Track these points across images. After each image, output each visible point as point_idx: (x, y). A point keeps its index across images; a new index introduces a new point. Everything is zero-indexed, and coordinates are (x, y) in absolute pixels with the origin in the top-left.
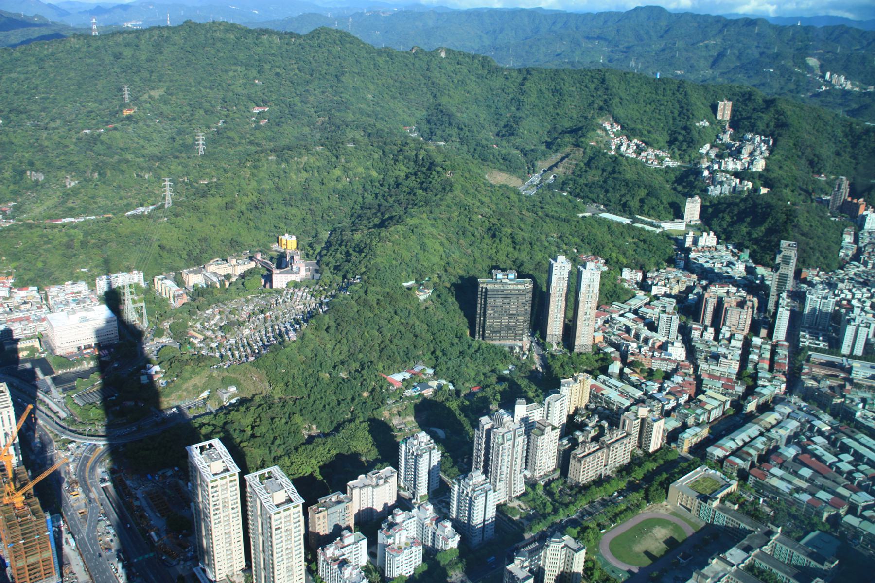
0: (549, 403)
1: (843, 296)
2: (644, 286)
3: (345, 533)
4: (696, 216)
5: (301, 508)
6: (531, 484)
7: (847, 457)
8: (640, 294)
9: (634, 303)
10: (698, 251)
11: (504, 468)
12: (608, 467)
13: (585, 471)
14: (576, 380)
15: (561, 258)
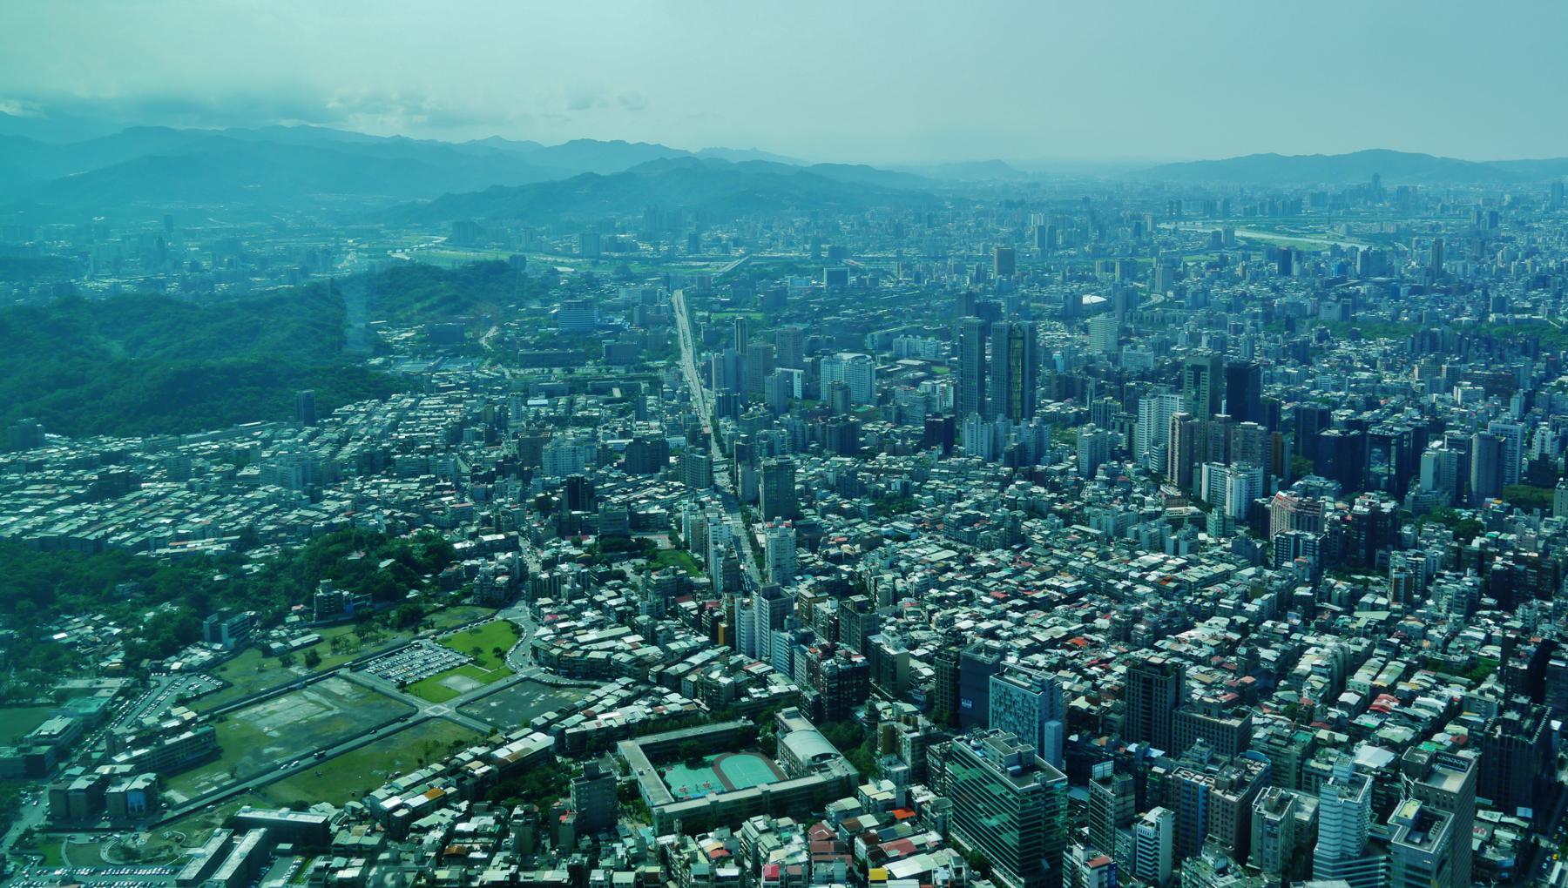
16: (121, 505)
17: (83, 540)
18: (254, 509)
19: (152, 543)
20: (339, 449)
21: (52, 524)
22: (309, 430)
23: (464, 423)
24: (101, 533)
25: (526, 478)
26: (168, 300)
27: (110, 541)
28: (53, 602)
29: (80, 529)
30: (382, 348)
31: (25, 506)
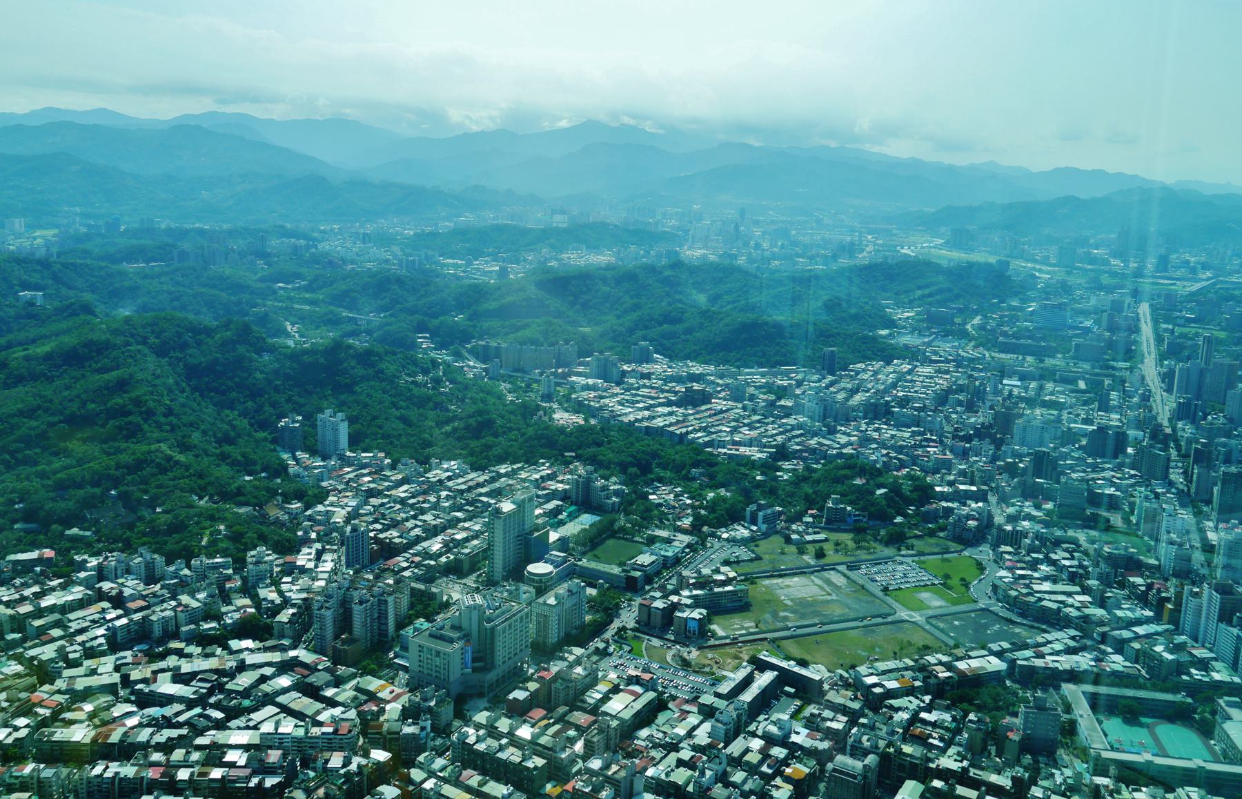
16: (697, 413)
17: (672, 433)
18: (787, 431)
19: (716, 443)
20: (851, 396)
21: (654, 418)
22: (830, 378)
23: (949, 391)
24: (684, 430)
25: (998, 444)
26: (739, 269)
27: (691, 436)
28: (651, 472)
29: (671, 425)
30: (891, 324)
31: (638, 402)
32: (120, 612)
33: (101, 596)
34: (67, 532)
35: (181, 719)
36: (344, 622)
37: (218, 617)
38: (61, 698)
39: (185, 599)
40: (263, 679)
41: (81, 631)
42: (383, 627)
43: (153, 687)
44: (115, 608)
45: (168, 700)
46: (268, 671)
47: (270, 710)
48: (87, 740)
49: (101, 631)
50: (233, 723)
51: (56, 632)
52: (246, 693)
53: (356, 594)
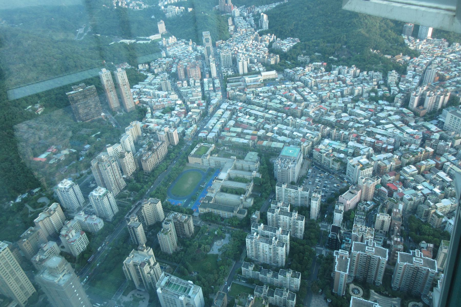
0: (124, 142)
1: (234, 49)
2: (150, 70)
3: (43, 245)
4: (164, 30)
5: (8, 249)
6: (127, 180)
7: (253, 118)
8: (149, 74)
9: (147, 80)
10: (169, 46)
11: (112, 180)
12: (160, 159)
13: (149, 166)
14: (132, 126)
15: (104, 70)
32: (345, 85)
33: (339, 79)
34: (330, 58)
35: (363, 121)
36: (421, 102)
37: (376, 93)
38: (329, 108)
39: (366, 85)
40: (390, 115)
41: (333, 89)
42: (436, 106)
43: (354, 110)
44: (343, 83)
45: (359, 115)
46: (392, 113)
47: (391, 125)
48: (334, 121)
49: (339, 90)
50: (378, 127)
51: (326, 88)
52: (383, 119)
53: (428, 93)
